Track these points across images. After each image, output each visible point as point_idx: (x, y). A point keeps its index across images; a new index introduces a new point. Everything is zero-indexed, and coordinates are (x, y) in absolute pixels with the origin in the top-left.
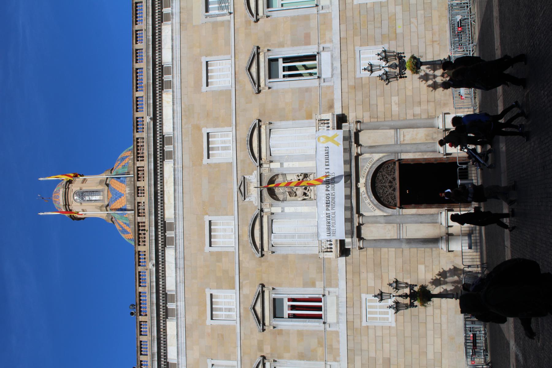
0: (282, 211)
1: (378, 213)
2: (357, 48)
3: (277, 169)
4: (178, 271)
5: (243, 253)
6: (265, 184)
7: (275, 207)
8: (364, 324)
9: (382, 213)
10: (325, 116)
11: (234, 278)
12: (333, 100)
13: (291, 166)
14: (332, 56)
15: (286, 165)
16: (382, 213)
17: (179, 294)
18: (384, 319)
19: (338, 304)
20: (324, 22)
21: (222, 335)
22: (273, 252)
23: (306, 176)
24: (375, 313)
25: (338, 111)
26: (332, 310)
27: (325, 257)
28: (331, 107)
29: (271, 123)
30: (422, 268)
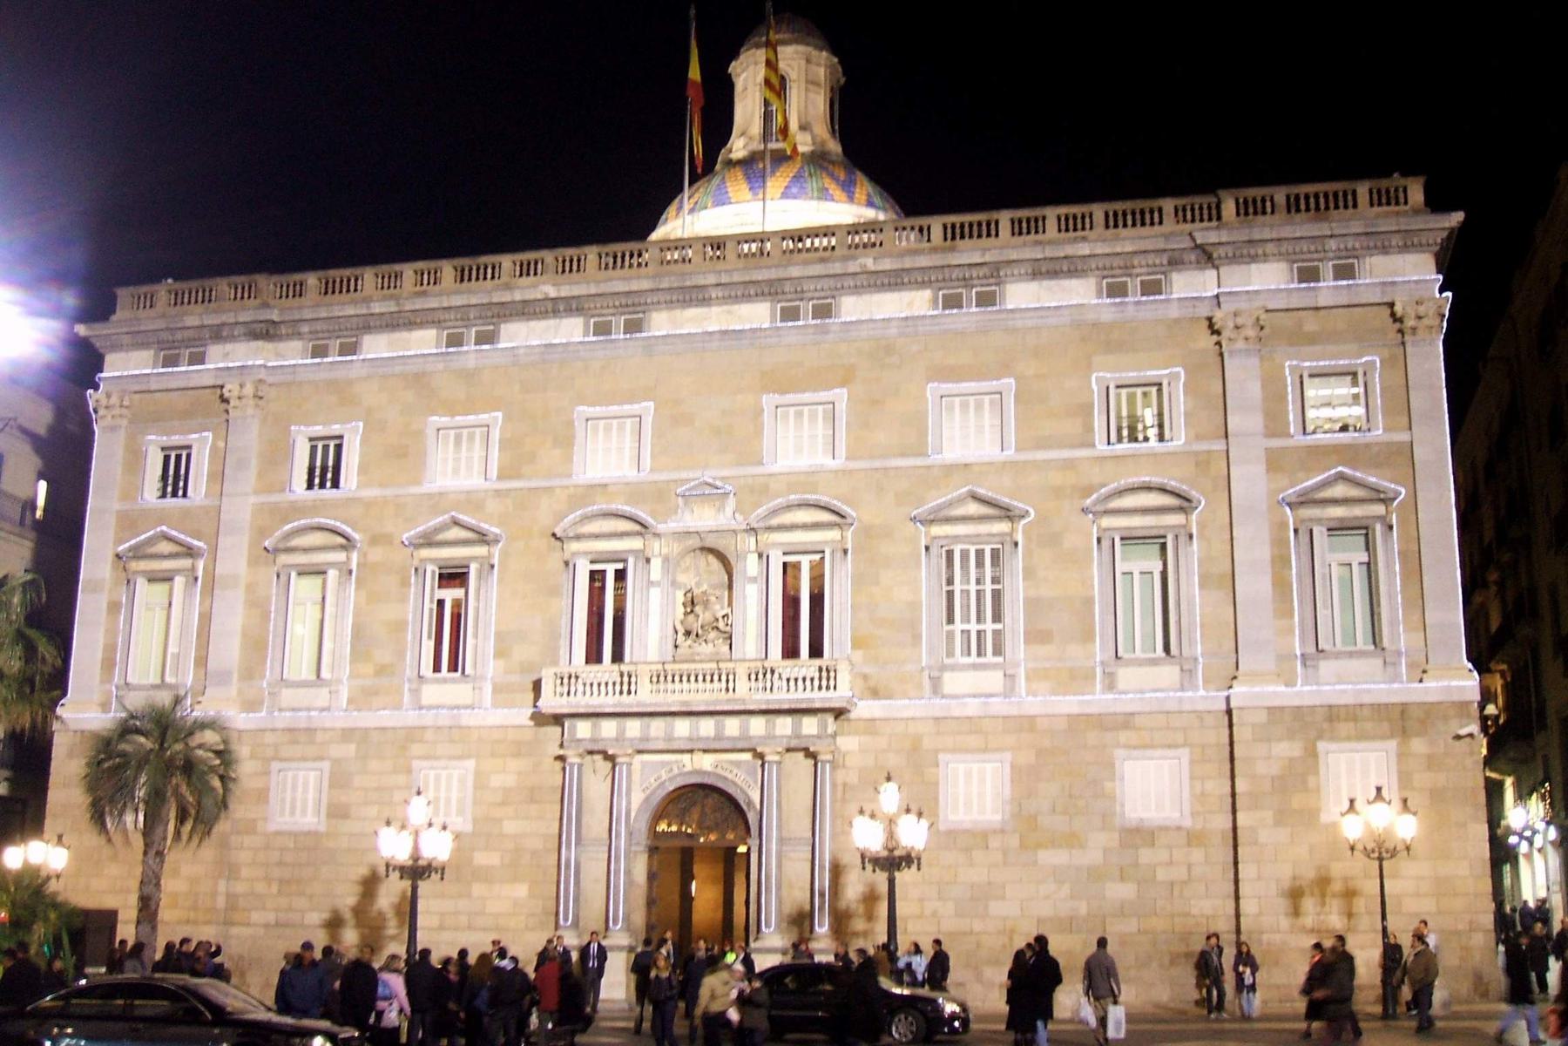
1: (637, 798)
2: (1008, 756)
6: (710, 542)
8: (416, 764)
9: (635, 806)
11: (519, 476)
12: (889, 697)
14: (991, 695)
16: (635, 806)
20: (1077, 679)
25: (865, 709)
26: (444, 691)
28: (875, 693)
30: (522, 890)
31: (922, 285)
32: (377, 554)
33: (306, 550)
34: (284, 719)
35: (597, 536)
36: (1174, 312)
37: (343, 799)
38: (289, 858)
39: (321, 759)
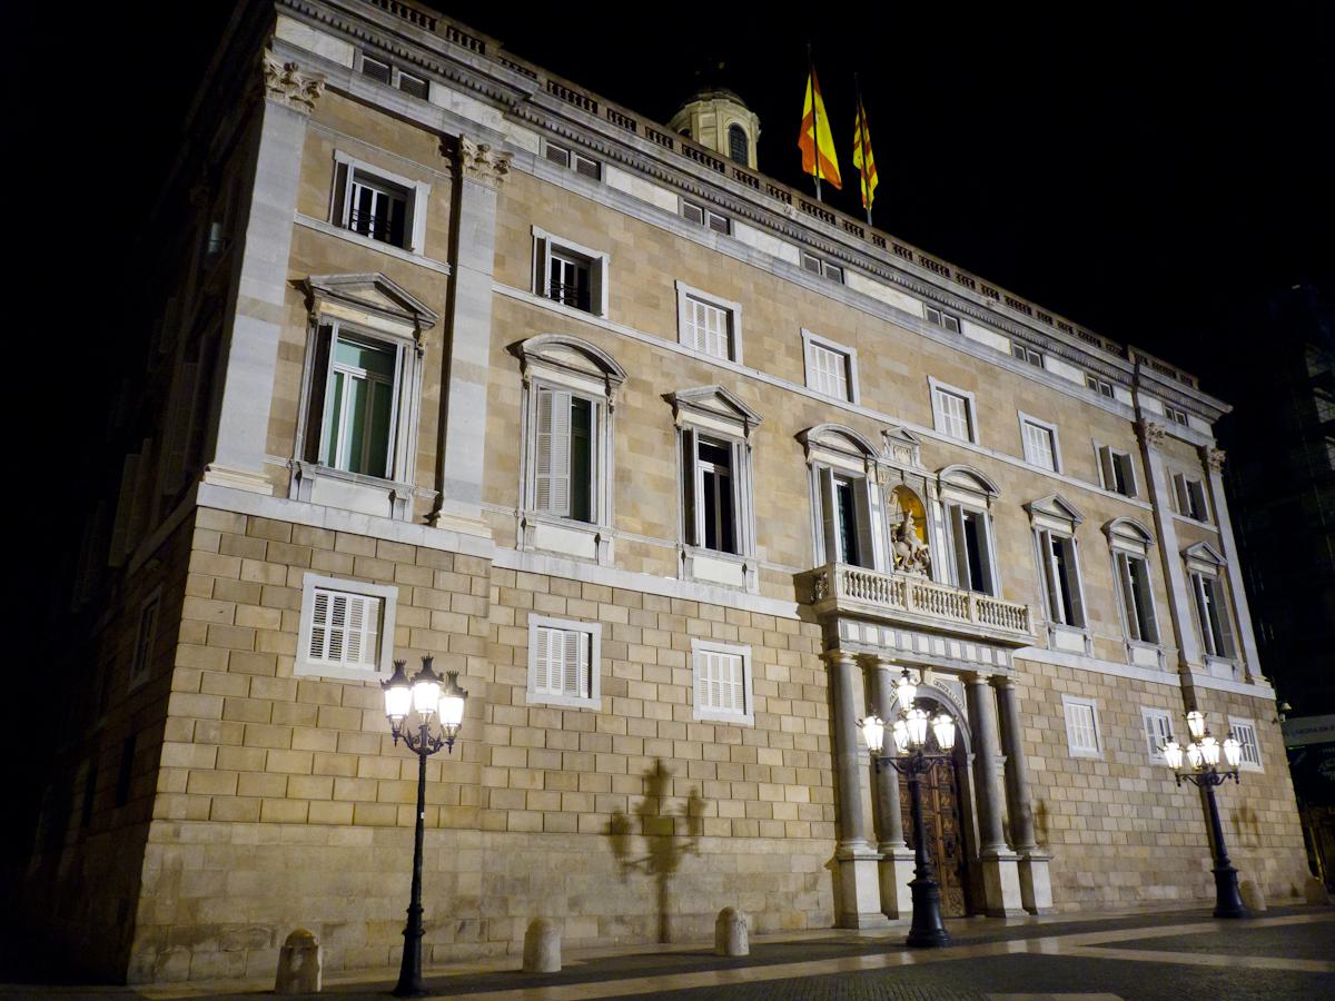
2: (1094, 703)
4: (767, 259)
8: (695, 643)
11: (760, 369)
14: (1080, 655)
17: (729, 244)
18: (705, 693)
19: (730, 587)
21: (656, 307)
24: (716, 675)
30: (801, 795)
31: (1009, 333)
32: (636, 400)
33: (560, 366)
34: (541, 565)
35: (833, 449)
36: (1119, 411)
37: (618, 673)
38: (557, 741)
39: (591, 620)
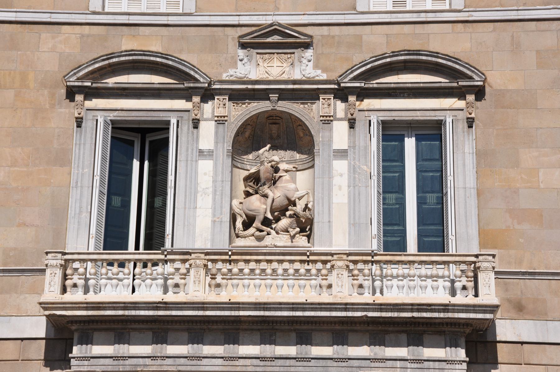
0: (201, 151)
3: (330, 141)
5: (83, 36)
7: (216, 133)
10: (487, 280)
13: (337, 181)
15: (340, 166)
22: (79, 122)
23: (305, 226)
25: (506, 330)
27: (48, 272)
28: (520, 309)
29: (470, 126)
